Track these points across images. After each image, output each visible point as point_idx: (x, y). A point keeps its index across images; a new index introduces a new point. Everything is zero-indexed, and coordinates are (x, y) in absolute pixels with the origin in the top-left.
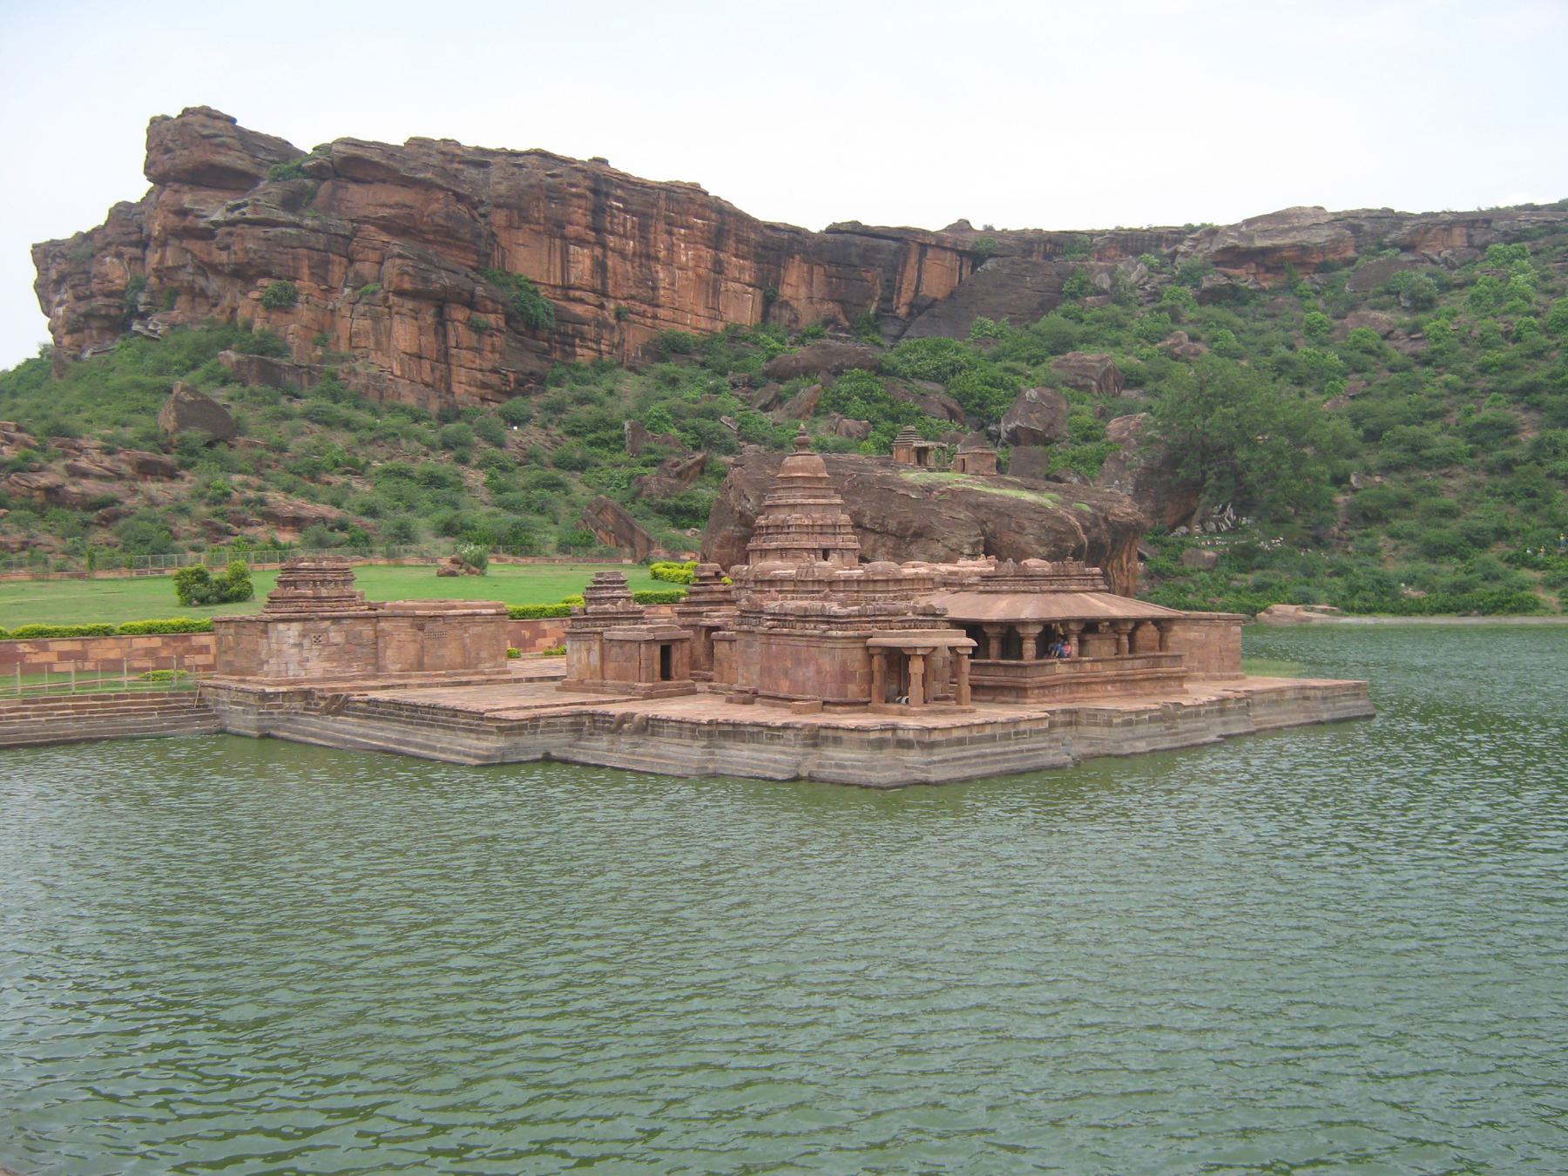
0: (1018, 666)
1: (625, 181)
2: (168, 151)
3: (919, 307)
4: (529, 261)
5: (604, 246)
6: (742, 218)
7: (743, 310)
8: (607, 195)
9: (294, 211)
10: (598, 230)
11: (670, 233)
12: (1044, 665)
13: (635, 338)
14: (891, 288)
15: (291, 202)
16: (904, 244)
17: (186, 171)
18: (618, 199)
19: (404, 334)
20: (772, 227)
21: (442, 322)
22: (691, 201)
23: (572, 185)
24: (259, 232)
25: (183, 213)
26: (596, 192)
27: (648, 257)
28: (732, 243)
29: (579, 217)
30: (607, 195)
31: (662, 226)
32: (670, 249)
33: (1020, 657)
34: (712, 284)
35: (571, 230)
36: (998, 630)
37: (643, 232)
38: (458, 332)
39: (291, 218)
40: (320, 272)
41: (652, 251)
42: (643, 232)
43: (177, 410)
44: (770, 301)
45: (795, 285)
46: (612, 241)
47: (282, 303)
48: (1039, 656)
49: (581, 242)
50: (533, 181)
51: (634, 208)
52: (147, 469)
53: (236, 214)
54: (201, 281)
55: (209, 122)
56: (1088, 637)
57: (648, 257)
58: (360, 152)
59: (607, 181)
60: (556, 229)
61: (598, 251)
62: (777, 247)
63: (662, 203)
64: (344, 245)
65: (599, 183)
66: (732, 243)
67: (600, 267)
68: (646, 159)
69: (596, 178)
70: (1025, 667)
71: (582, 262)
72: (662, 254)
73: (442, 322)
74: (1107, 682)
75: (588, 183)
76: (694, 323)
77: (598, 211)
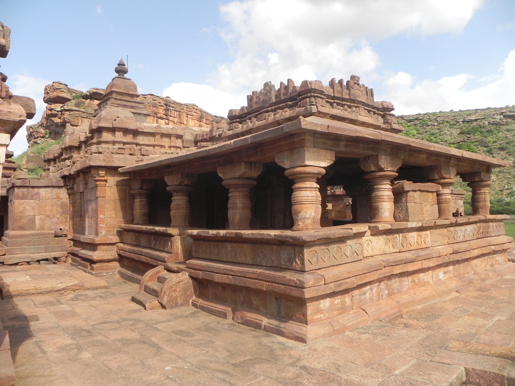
0: (281, 243)
1: (174, 103)
2: (48, 93)
5: (168, 120)
6: (207, 113)
8: (170, 106)
9: (78, 107)
10: (167, 115)
11: (187, 117)
12: (342, 240)
17: (53, 98)
18: (172, 107)
20: (216, 117)
22: (193, 108)
23: (159, 103)
24: (68, 113)
25: (51, 110)
26: (166, 105)
28: (204, 120)
29: (161, 112)
30: (170, 106)
31: (185, 115)
32: (187, 121)
33: (289, 221)
35: (159, 115)
36: (241, 170)
37: (180, 116)
39: (77, 109)
41: (182, 122)
43: (27, 158)
46: (171, 118)
48: (326, 220)
49: (162, 118)
50: (148, 102)
51: (177, 110)
53: (63, 108)
54: (57, 129)
55: (59, 85)
56: (408, 185)
57: (181, 123)
58: (97, 91)
59: (169, 102)
61: (167, 121)
63: (185, 109)
66: (204, 120)
69: (166, 101)
70: (299, 245)
72: (185, 122)
74: (439, 266)
75: (165, 102)
77: (167, 110)
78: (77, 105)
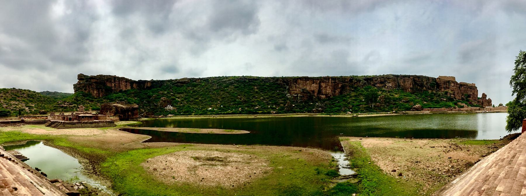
1: (118, 78)
3: (147, 87)
4: (109, 85)
7: (129, 88)
13: (118, 91)
14: (144, 86)
15: (86, 81)
16: (145, 82)
19: (95, 92)
21: (99, 91)
27: (119, 84)
34: (126, 86)
37: (119, 82)
38: (100, 92)
40: (89, 87)
42: (119, 82)
44: (132, 87)
45: (134, 85)
47: (85, 90)
52: (70, 104)
60: (111, 82)
62: (132, 82)
64: (91, 85)
65: (115, 77)
67: (115, 85)
68: (120, 75)
71: (113, 85)
73: (99, 91)
76: (124, 89)
78: (86, 81)
